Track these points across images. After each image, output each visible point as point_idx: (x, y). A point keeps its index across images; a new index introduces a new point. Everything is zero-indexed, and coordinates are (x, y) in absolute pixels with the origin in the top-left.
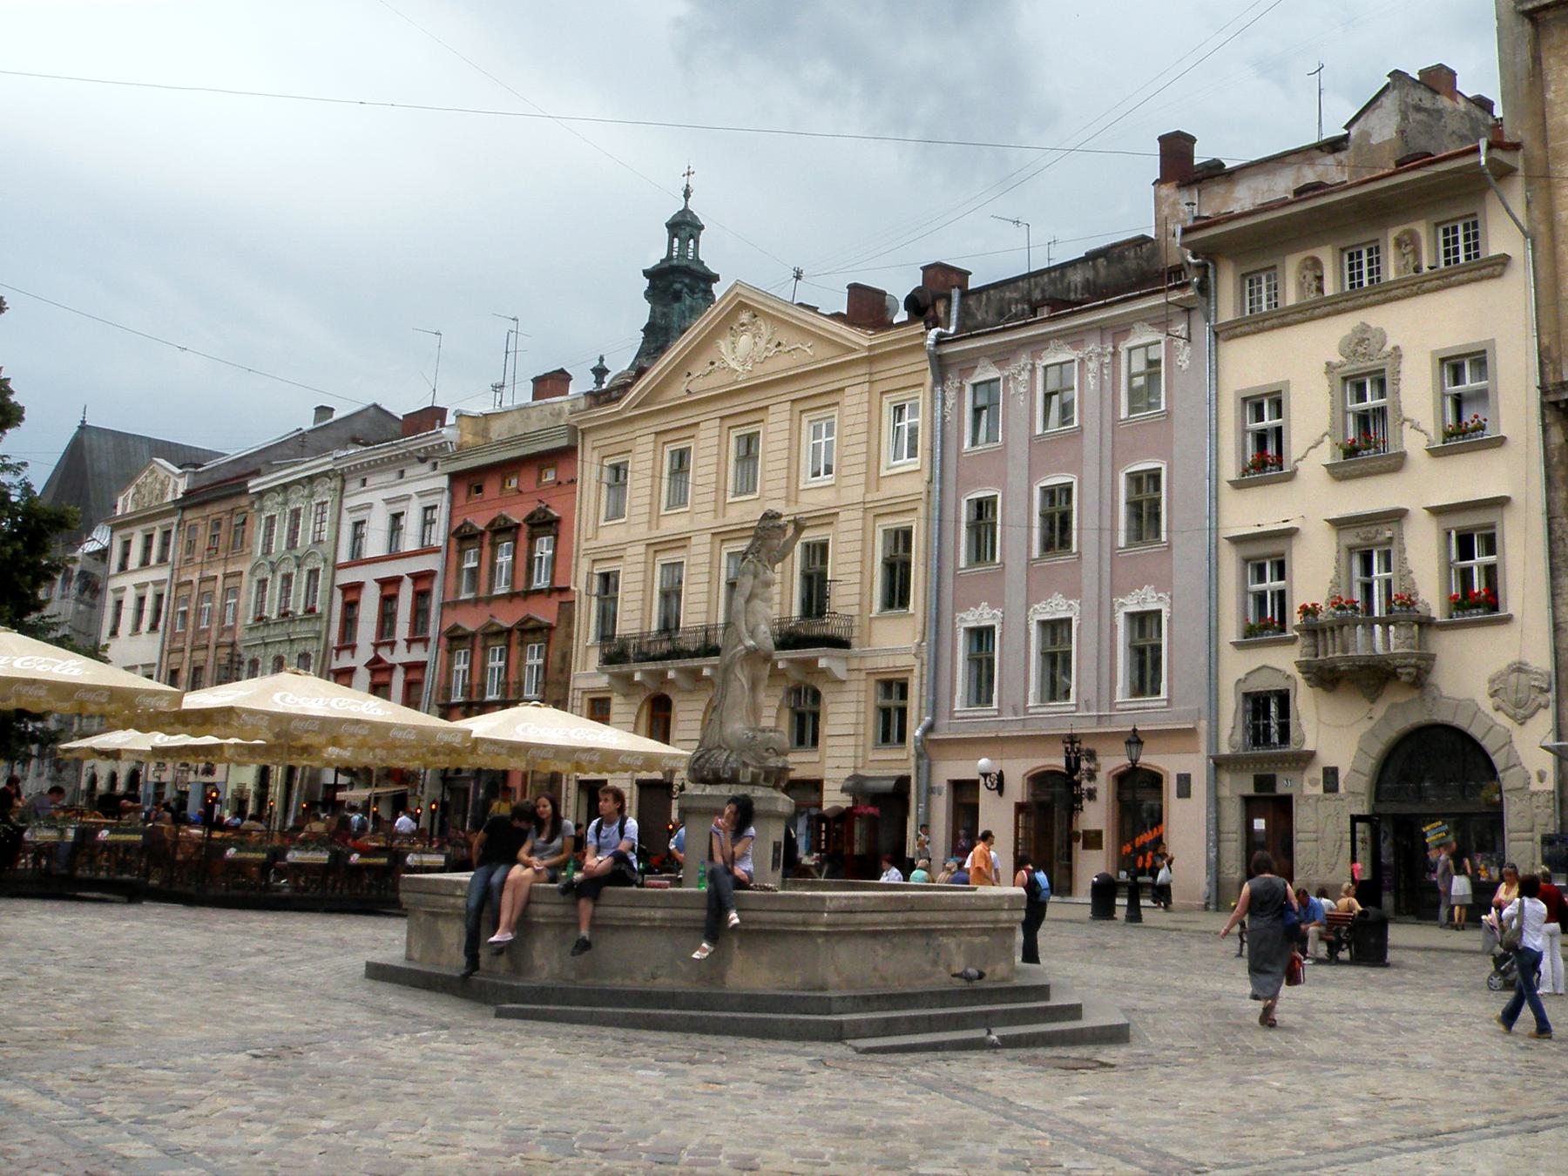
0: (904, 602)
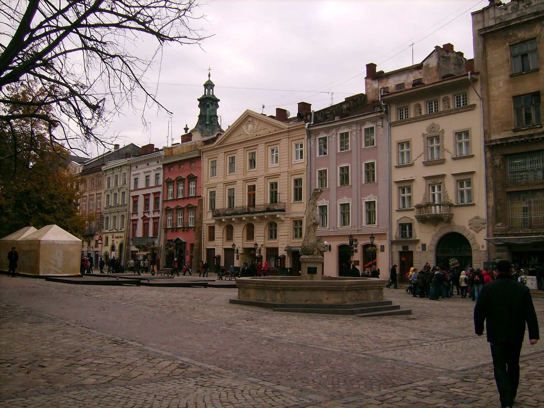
0: (300, 199)
